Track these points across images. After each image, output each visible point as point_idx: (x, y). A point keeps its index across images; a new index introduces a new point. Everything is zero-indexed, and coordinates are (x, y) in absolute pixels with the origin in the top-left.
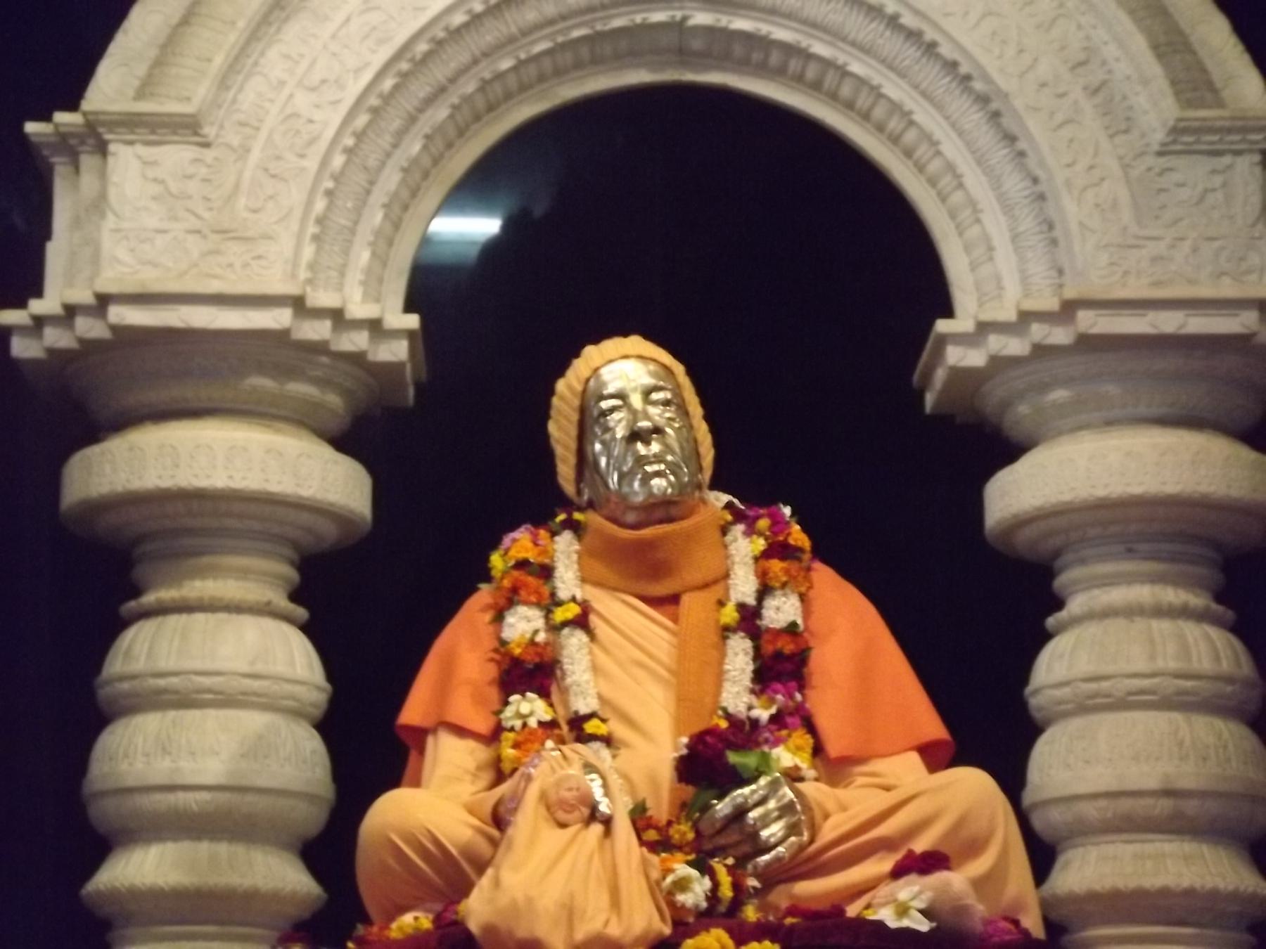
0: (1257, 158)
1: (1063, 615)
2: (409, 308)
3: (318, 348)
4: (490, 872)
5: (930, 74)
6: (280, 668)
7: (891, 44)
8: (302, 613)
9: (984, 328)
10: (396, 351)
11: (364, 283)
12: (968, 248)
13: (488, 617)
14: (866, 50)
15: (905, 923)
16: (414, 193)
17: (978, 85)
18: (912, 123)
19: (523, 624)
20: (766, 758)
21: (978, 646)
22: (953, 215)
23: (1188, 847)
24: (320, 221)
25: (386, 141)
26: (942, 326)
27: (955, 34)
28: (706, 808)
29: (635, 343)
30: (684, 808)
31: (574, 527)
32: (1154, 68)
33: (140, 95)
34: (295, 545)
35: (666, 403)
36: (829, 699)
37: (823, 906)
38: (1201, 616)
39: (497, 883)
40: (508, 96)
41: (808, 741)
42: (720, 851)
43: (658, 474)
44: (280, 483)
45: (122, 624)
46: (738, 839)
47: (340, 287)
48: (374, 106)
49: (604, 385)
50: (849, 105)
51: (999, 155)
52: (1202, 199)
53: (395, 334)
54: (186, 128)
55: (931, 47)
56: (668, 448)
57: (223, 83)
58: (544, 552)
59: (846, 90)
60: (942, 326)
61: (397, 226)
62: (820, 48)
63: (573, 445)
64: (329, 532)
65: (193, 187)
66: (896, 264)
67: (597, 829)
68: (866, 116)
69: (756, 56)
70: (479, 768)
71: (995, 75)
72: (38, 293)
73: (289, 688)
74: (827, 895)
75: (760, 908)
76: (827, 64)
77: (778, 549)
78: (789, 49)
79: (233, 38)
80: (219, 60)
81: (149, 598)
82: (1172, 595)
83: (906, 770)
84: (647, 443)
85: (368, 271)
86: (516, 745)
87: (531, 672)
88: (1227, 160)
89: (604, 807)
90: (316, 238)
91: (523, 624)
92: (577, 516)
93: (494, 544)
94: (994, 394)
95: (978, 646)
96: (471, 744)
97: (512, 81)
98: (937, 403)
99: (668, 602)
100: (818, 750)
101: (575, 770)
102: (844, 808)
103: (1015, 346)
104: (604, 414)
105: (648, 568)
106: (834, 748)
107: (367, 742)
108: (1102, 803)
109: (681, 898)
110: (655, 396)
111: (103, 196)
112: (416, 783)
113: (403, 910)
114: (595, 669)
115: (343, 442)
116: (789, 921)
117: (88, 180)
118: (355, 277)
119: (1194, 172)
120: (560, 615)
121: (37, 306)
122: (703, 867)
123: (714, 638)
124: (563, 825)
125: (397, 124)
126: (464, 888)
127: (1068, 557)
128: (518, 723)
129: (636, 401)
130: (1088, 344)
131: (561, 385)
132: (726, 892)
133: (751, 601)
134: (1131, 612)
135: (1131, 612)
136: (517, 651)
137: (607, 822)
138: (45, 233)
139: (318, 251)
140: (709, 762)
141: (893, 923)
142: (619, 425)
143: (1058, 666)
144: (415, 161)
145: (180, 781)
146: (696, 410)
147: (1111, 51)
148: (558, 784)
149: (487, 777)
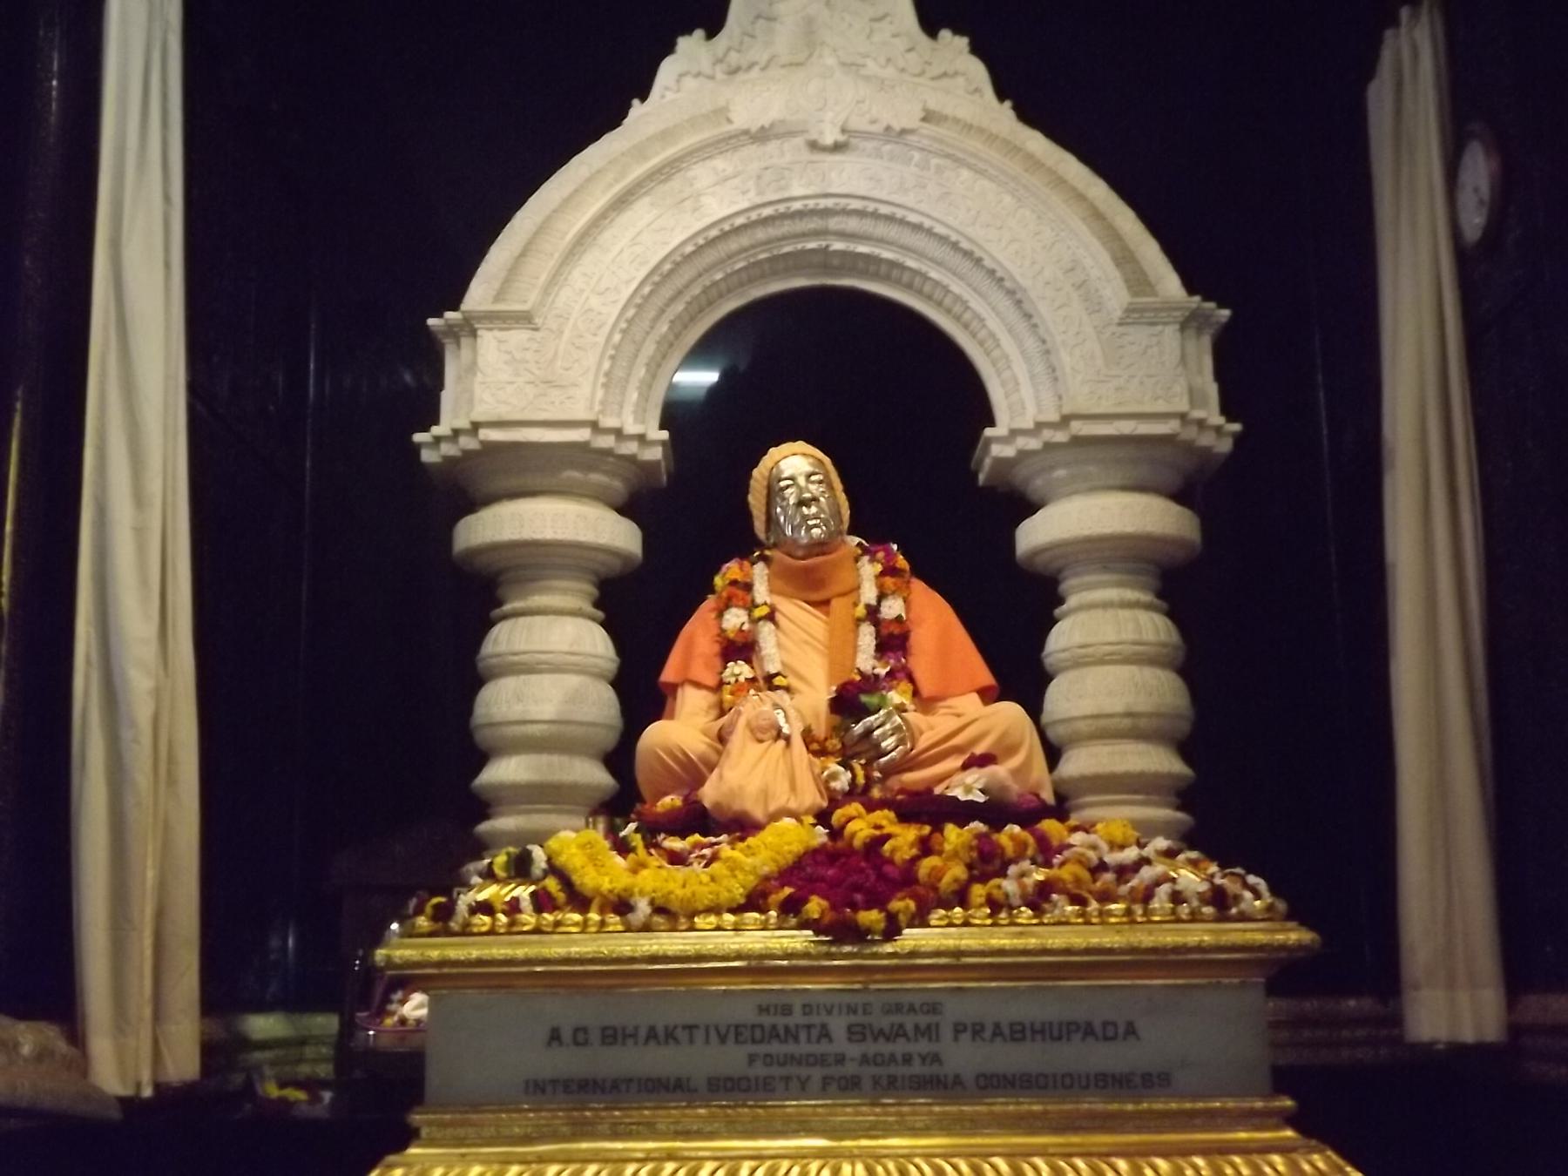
0: (1177, 327)
1: (1065, 607)
2: (662, 427)
3: (608, 452)
4: (716, 771)
5: (978, 277)
6: (588, 648)
7: (956, 260)
8: (600, 614)
9: (1014, 433)
10: (655, 454)
11: (635, 412)
12: (1003, 384)
13: (713, 615)
14: (939, 264)
15: (970, 797)
16: (664, 357)
17: (1008, 284)
18: (968, 308)
19: (735, 619)
20: (884, 698)
21: (1012, 629)
22: (994, 364)
23: (1142, 747)
24: (607, 374)
25: (646, 324)
26: (988, 432)
27: (995, 254)
28: (848, 729)
29: (800, 446)
30: (835, 730)
31: (763, 558)
32: (1115, 274)
33: (498, 298)
34: (596, 573)
35: (820, 482)
36: (922, 660)
37: (921, 787)
38: (1148, 607)
39: (721, 777)
40: (721, 296)
41: (910, 687)
42: (857, 755)
43: (815, 526)
44: (586, 536)
45: (492, 624)
46: (868, 747)
47: (619, 415)
48: (639, 302)
49: (781, 472)
50: (929, 298)
51: (1021, 326)
52: (1145, 352)
53: (653, 443)
54: (524, 319)
55: (978, 261)
56: (821, 510)
57: (546, 291)
58: (747, 575)
59: (927, 288)
60: (989, 432)
61: (654, 376)
62: (911, 263)
63: (764, 509)
64: (616, 565)
65: (529, 355)
66: (959, 393)
67: (782, 743)
68: (939, 304)
69: (872, 268)
70: (710, 707)
71: (1018, 278)
72: (437, 422)
73: (592, 660)
74: (923, 780)
75: (884, 789)
76: (915, 272)
77: (890, 571)
78: (893, 264)
79: (552, 264)
80: (543, 278)
81: (507, 607)
82: (1131, 595)
83: (970, 704)
84: (809, 506)
85: (637, 404)
86: (732, 693)
87: (740, 648)
88: (1160, 328)
89: (786, 730)
90: (605, 385)
91: (735, 619)
92: (767, 553)
93: (717, 570)
94: (1021, 473)
95: (1012, 629)
96: (704, 693)
97: (723, 286)
98: (987, 479)
99: (823, 604)
100: (916, 693)
101: (767, 708)
102: (932, 728)
103: (1033, 444)
104: (783, 489)
105: (811, 581)
106: (927, 689)
107: (642, 695)
108: (1089, 722)
109: (833, 784)
110: (813, 478)
111: (474, 363)
112: (671, 717)
113: (666, 794)
114: (779, 645)
115: (623, 510)
116: (900, 797)
117: (465, 352)
118: (629, 409)
119: (1139, 336)
120: (758, 613)
121: (435, 430)
122: (846, 765)
123: (851, 626)
124: (761, 741)
125: (652, 314)
126: (700, 781)
127: (1066, 573)
128: (733, 680)
129: (802, 481)
130: (1078, 441)
131: (755, 472)
132: (861, 780)
133: (874, 602)
134: (1106, 605)
135: (1106, 605)
136: (731, 635)
137: (788, 739)
138: (439, 384)
139: (606, 393)
140: (849, 701)
141: (962, 798)
142: (791, 496)
143: (1062, 639)
144: (664, 337)
145: (528, 718)
146: (838, 485)
147: (1088, 262)
148: (757, 717)
149: (714, 713)
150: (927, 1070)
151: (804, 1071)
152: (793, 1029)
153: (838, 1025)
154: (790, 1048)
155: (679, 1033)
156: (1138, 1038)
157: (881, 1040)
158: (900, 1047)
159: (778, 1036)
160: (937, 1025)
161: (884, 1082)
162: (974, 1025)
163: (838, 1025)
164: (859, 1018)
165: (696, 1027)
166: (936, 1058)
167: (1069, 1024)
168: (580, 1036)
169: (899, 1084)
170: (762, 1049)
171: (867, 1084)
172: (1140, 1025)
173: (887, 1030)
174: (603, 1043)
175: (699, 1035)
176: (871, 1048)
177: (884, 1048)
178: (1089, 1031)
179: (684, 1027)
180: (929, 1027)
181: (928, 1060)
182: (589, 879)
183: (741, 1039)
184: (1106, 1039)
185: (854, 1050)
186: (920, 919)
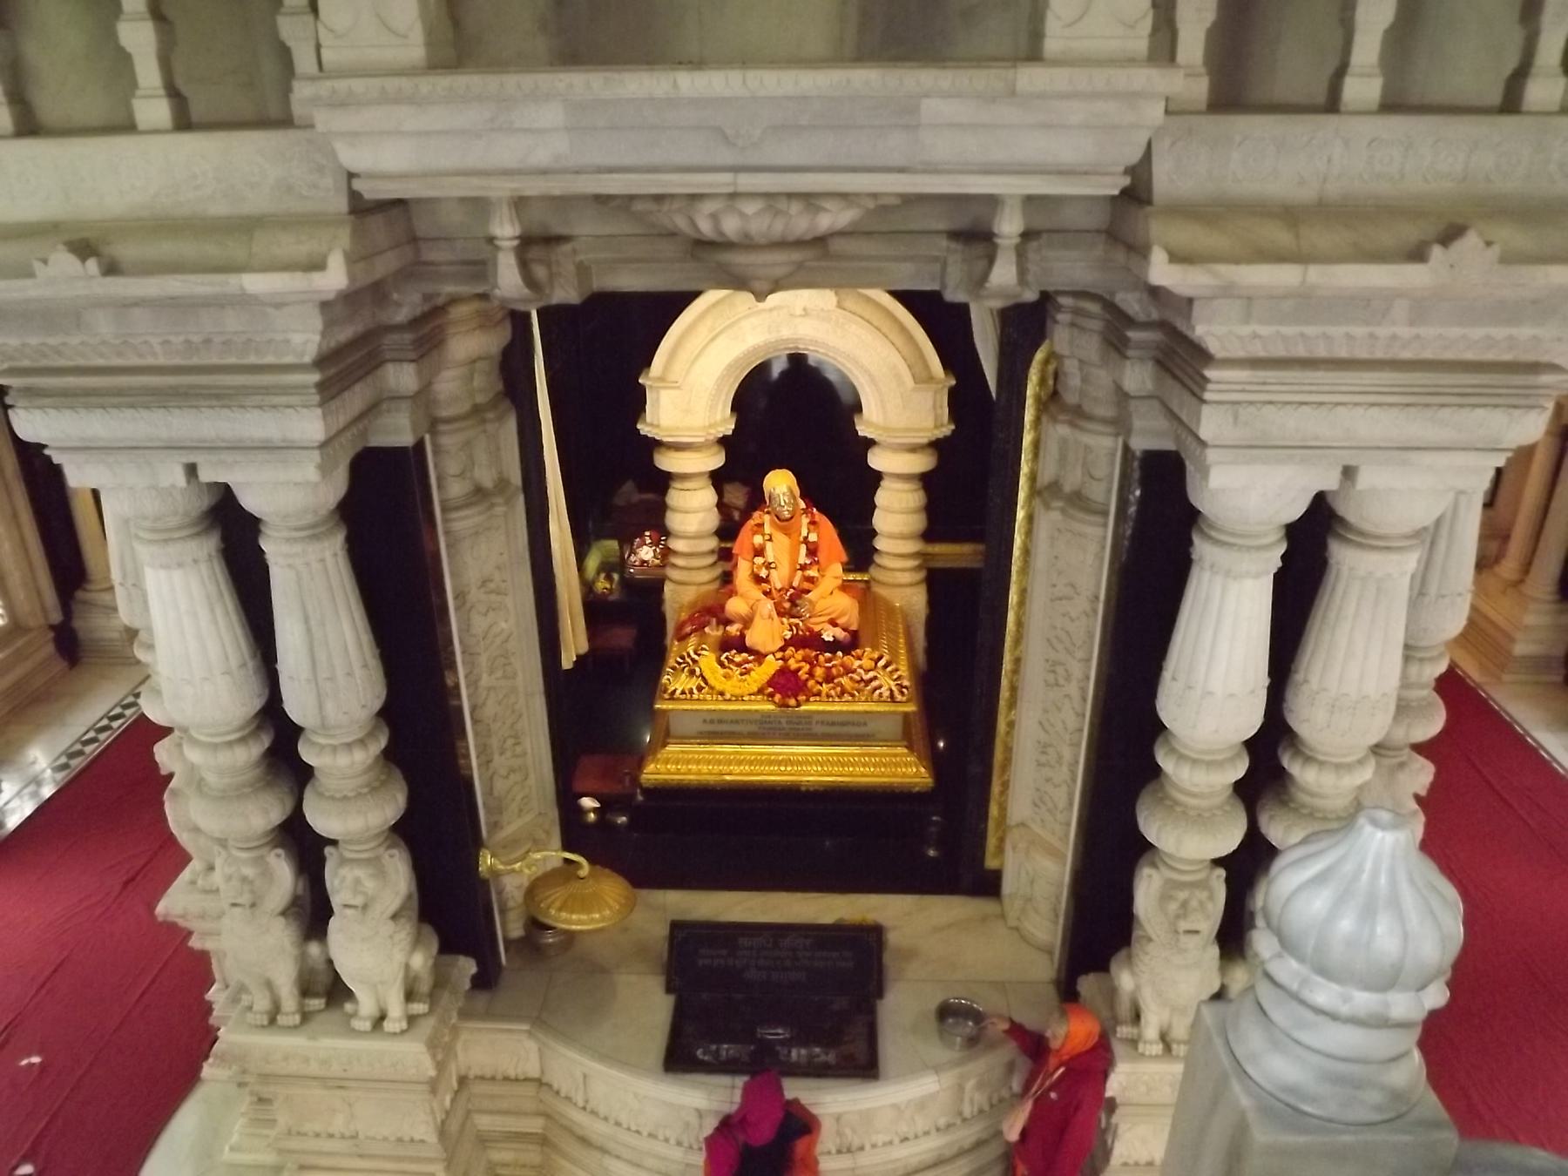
19: (758, 539)
36: (821, 556)
87: (759, 552)
91: (758, 539)
105: (785, 524)
153: (783, 721)
163: (783, 721)
168: (712, 721)
182: (712, 681)
186: (808, 700)
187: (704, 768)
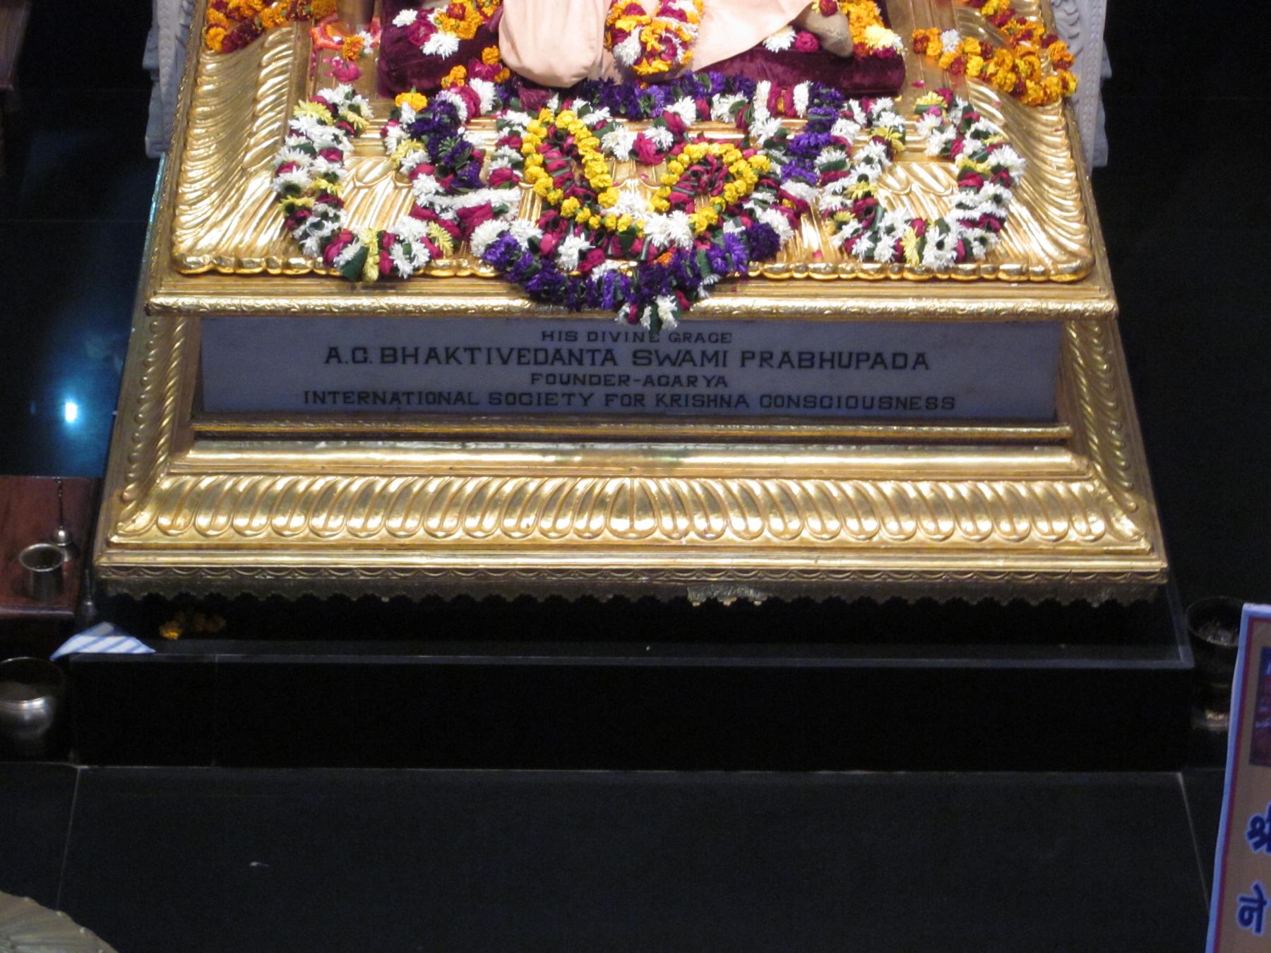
150: (711, 391)
151: (587, 390)
152: (577, 354)
153: (623, 351)
154: (574, 369)
155: (461, 355)
156: (927, 368)
157: (667, 363)
158: (686, 370)
159: (561, 359)
160: (725, 353)
161: (667, 400)
162: (762, 353)
163: (623, 351)
164: (647, 345)
165: (479, 349)
166: (722, 381)
167: (858, 355)
168: (360, 355)
169: (682, 402)
170: (546, 369)
171: (650, 402)
172: (930, 357)
173: (673, 356)
174: (383, 362)
175: (481, 357)
176: (655, 370)
177: (668, 369)
178: (879, 360)
179: (465, 349)
180: (716, 353)
181: (714, 382)
183: (523, 360)
184: (894, 367)
185: (640, 373)
187: (335, 525)
